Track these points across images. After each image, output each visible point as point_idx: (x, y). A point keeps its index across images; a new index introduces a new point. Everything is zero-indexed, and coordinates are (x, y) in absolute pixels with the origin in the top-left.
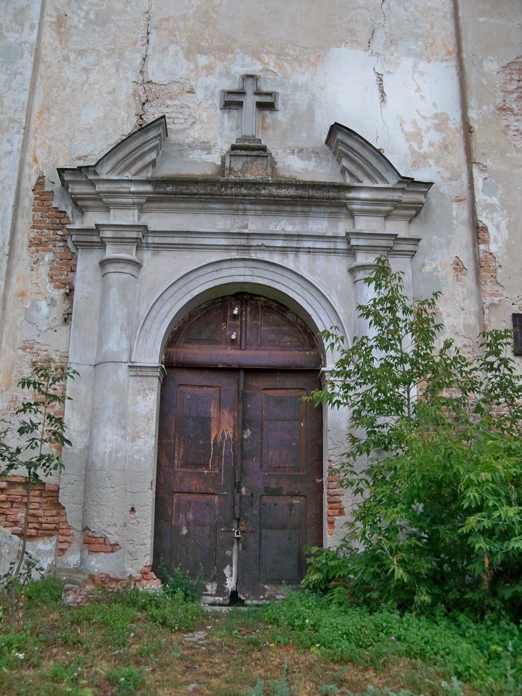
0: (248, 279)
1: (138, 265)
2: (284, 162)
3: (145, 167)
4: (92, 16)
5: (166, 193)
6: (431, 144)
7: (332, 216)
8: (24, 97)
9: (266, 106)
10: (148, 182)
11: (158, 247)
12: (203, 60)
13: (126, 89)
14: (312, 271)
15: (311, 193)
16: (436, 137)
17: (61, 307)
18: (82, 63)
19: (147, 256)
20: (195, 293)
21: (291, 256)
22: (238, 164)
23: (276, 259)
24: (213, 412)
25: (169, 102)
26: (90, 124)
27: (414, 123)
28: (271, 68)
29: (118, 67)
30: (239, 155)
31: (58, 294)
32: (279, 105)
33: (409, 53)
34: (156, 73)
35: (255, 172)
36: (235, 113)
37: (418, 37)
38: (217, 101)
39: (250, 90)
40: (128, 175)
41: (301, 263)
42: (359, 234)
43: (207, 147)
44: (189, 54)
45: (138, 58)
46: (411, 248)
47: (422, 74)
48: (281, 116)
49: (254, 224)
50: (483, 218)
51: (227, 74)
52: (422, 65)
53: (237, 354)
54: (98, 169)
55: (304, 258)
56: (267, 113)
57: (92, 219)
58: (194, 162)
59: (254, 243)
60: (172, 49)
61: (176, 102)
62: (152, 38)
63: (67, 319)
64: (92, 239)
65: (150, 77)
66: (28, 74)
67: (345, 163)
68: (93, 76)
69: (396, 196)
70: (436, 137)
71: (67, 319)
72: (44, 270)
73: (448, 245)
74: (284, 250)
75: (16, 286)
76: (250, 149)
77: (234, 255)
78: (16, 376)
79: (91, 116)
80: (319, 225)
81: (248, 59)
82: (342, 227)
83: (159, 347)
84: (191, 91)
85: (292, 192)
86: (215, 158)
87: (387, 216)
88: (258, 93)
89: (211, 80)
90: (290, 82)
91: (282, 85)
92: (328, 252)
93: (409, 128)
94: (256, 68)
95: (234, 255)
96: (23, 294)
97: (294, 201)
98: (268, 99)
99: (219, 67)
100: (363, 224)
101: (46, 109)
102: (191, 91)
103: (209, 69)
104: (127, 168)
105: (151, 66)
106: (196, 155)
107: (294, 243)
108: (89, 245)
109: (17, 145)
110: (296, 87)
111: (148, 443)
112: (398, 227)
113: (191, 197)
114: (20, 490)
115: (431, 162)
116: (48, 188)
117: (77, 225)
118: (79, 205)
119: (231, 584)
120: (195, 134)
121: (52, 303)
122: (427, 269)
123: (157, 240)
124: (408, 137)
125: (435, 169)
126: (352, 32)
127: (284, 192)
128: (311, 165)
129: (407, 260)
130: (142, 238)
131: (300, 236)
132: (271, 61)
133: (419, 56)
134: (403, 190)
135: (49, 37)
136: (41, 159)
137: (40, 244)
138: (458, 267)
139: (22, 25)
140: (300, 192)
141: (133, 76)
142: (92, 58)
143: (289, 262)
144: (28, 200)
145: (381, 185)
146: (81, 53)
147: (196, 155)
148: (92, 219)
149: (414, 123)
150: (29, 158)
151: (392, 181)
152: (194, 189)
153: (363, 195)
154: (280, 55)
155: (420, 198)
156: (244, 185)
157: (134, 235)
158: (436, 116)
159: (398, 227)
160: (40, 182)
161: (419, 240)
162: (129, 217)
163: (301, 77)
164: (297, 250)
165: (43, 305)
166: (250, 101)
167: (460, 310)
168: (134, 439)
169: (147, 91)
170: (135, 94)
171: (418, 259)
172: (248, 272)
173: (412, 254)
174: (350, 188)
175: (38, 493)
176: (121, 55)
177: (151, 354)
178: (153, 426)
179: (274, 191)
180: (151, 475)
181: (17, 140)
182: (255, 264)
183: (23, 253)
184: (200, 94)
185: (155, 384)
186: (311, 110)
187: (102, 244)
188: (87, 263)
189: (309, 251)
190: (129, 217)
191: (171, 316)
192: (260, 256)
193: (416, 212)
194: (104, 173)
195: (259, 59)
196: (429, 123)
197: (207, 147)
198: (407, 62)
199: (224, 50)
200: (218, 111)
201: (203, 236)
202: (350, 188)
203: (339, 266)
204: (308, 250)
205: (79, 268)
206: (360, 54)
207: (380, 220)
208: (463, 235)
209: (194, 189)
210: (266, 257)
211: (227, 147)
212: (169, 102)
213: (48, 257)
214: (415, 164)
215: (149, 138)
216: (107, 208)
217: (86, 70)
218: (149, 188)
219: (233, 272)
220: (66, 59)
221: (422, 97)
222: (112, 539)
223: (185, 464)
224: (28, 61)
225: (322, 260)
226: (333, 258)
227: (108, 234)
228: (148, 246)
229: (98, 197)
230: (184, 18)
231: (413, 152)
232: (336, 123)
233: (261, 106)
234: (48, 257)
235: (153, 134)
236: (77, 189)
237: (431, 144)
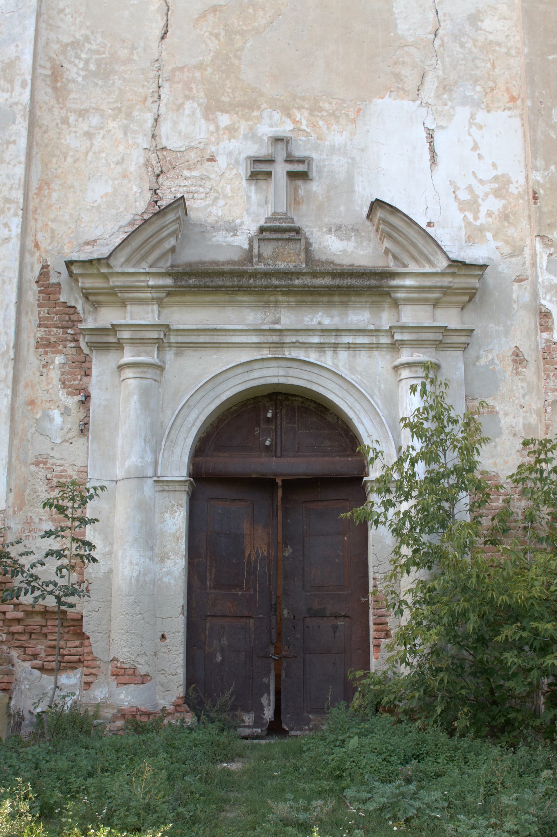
0: (282, 380)
1: (160, 368)
2: (320, 244)
3: (164, 255)
4: (92, 67)
5: (189, 286)
6: (490, 214)
7: (375, 306)
8: (20, 171)
9: (299, 176)
10: (168, 274)
11: (182, 348)
12: (224, 120)
13: (136, 159)
14: (352, 369)
15: (349, 281)
16: (494, 204)
17: (77, 415)
18: (84, 127)
19: (170, 356)
20: (224, 397)
21: (329, 353)
22: (268, 250)
23: (313, 357)
24: (246, 528)
25: (186, 173)
26: (99, 208)
27: (470, 189)
28: (304, 127)
29: (126, 130)
30: (268, 239)
31: (72, 401)
32: (314, 174)
33: (465, 101)
34: (170, 138)
35: (288, 259)
36: (262, 183)
37: (476, 81)
38: (243, 171)
39: (281, 156)
40: (144, 267)
41: (340, 361)
42: (404, 328)
44: (209, 112)
45: (149, 118)
46: (463, 339)
47: (480, 127)
48: (316, 187)
49: (288, 319)
50: (547, 303)
51: (253, 136)
52: (481, 116)
53: (271, 470)
54: (112, 262)
55: (343, 355)
56: (300, 183)
57: (108, 316)
58: (219, 246)
59: (288, 339)
60: (188, 106)
61: (195, 173)
62: (164, 92)
63: (84, 429)
64: (107, 340)
65: (164, 142)
66: (23, 142)
67: (387, 244)
68: (98, 141)
69: (446, 281)
70: (494, 204)
71: (84, 429)
72: (55, 374)
73: (507, 333)
74: (321, 347)
75: (24, 394)
76: (281, 231)
77: (266, 353)
78: (29, 494)
79: (98, 191)
80: (359, 317)
81: (277, 116)
82: (386, 319)
83: (186, 458)
84: (212, 159)
85: (328, 281)
87: (436, 304)
88: (290, 160)
89: (234, 145)
90: (327, 144)
91: (316, 147)
92: (370, 347)
93: (464, 195)
94: (285, 128)
95: (266, 353)
96: (32, 403)
97: (330, 291)
98: (300, 168)
99: (243, 127)
100: (410, 315)
101: (45, 184)
102: (212, 159)
103: (232, 130)
104: (144, 258)
105: (165, 128)
108: (104, 347)
109: (16, 230)
110: (333, 150)
111: (176, 566)
112: (449, 318)
113: (217, 290)
114: (38, 619)
115: (489, 235)
116: (53, 280)
117: (90, 324)
119: (269, 714)
121: (66, 412)
122: (482, 362)
123: (180, 339)
124: (463, 206)
125: (493, 244)
126: (398, 77)
127: (319, 281)
128: (350, 246)
129: (459, 353)
130: (163, 338)
131: (338, 331)
132: (302, 116)
133: (477, 104)
134: (453, 274)
135: (45, 95)
136: (43, 245)
137: (49, 344)
138: (518, 359)
139: (11, 82)
140: (337, 282)
141: (144, 142)
142: (95, 120)
143: (327, 360)
144: (32, 294)
145: (428, 269)
146: (82, 113)
147: (220, 238)
148: (108, 316)
149: (470, 189)
150: (30, 244)
151: (442, 264)
152: (219, 282)
153: (408, 282)
154: (314, 109)
155: (474, 282)
157: (155, 335)
158: (496, 179)
159: (449, 318)
160: (45, 272)
161: (472, 331)
162: (147, 315)
163: (337, 137)
164: (335, 346)
165: (56, 414)
166: (280, 170)
167: (519, 408)
168: (162, 561)
170: (147, 164)
171: (472, 352)
172: (281, 372)
173: (465, 346)
174: (393, 275)
175: (56, 622)
176: (129, 115)
177: (178, 468)
178: (182, 546)
179: (308, 281)
180: (181, 599)
181: (16, 223)
182: (289, 364)
184: (222, 161)
185: (183, 499)
186: (350, 179)
187: (119, 346)
188: (102, 366)
189: (349, 346)
190: (147, 315)
191: (199, 424)
192: (295, 354)
193: (470, 298)
194: (118, 264)
195: (289, 116)
196: (487, 188)
198: (462, 113)
199: (248, 105)
200: (244, 183)
201: (231, 334)
202: (393, 275)
203: (381, 363)
204: (347, 346)
205: (94, 372)
206: (407, 105)
207: (429, 308)
208: (524, 321)
209: (219, 282)
210: (301, 355)
211: (254, 228)
212: (186, 173)
213: (59, 359)
214: (470, 239)
215: (167, 222)
216: (123, 304)
217: (89, 135)
218: (169, 281)
219: (265, 372)
220: (65, 121)
221: (480, 157)
222: (142, 670)
223: (218, 586)
224: (20, 127)
225: (363, 358)
226: (376, 353)
227: (126, 335)
228: (170, 345)
229: (112, 292)
230: (200, 66)
231: (468, 224)
232: (377, 200)
233: (292, 175)
234: (59, 359)
235: (171, 217)
236: (89, 283)
237: (490, 214)
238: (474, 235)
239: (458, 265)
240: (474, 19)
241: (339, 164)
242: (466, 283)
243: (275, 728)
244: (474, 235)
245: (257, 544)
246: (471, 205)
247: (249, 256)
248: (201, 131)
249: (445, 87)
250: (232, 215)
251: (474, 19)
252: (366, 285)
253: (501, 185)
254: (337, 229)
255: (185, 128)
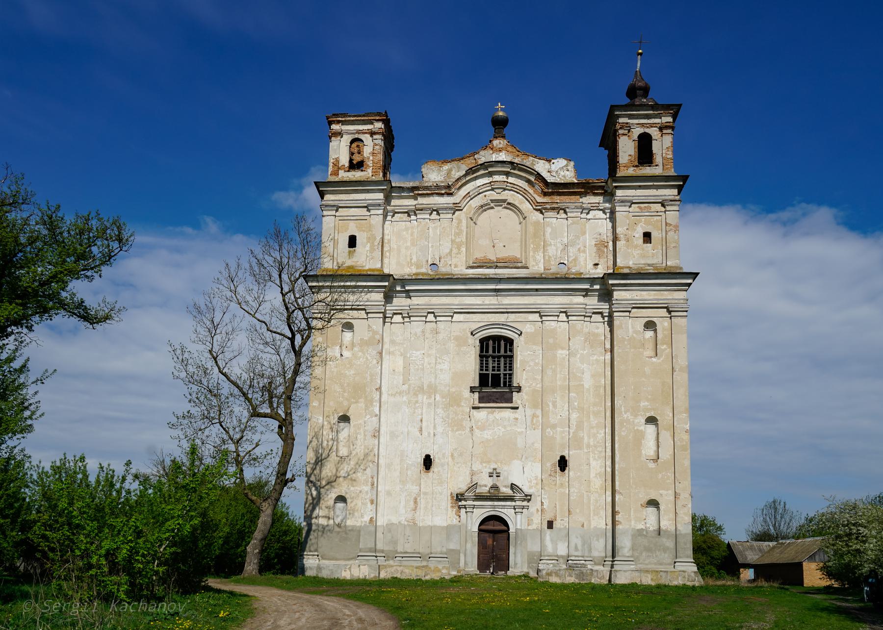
13: (468, 473)
16: (535, 482)
43: (486, 486)
44: (481, 463)
48: (501, 478)
49: (496, 503)
82: (513, 504)
86: (487, 489)
90: (503, 469)
94: (496, 466)
106: (484, 488)
107: (504, 507)
118: (460, 500)
120: (483, 483)
130: (474, 507)
138: (538, 510)
144: (449, 498)
148: (463, 503)
156: (494, 496)
159: (525, 503)
166: (495, 475)
169: (473, 474)
183: (450, 509)
188: (463, 510)
197: (486, 486)
199: (489, 462)
224: (446, 467)
238: (531, 487)
239: (526, 496)
240: (533, 444)
241: (505, 473)
242: (528, 498)
243: (492, 574)
244: (531, 487)
245: (490, 542)
246: (530, 482)
247: (489, 492)
248: (480, 467)
249: (526, 458)
250: (485, 484)
251: (533, 444)
252: (511, 499)
253: (536, 478)
254: (505, 486)
255: (477, 467)
